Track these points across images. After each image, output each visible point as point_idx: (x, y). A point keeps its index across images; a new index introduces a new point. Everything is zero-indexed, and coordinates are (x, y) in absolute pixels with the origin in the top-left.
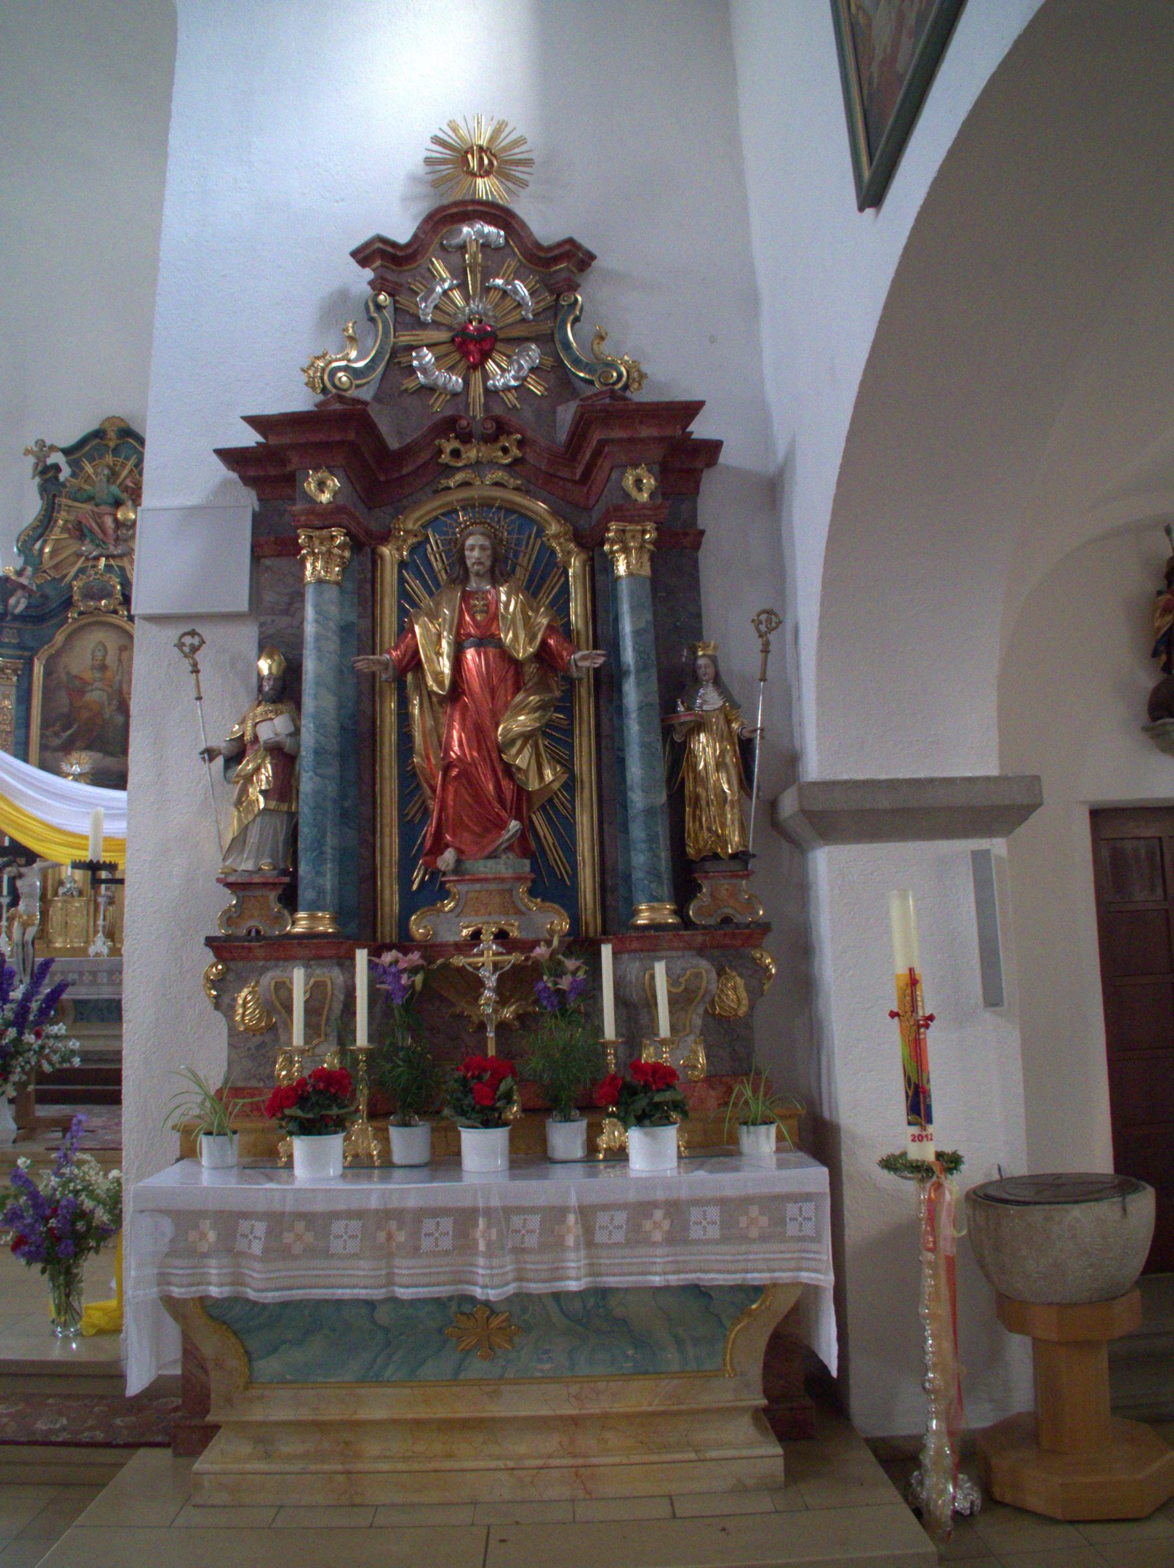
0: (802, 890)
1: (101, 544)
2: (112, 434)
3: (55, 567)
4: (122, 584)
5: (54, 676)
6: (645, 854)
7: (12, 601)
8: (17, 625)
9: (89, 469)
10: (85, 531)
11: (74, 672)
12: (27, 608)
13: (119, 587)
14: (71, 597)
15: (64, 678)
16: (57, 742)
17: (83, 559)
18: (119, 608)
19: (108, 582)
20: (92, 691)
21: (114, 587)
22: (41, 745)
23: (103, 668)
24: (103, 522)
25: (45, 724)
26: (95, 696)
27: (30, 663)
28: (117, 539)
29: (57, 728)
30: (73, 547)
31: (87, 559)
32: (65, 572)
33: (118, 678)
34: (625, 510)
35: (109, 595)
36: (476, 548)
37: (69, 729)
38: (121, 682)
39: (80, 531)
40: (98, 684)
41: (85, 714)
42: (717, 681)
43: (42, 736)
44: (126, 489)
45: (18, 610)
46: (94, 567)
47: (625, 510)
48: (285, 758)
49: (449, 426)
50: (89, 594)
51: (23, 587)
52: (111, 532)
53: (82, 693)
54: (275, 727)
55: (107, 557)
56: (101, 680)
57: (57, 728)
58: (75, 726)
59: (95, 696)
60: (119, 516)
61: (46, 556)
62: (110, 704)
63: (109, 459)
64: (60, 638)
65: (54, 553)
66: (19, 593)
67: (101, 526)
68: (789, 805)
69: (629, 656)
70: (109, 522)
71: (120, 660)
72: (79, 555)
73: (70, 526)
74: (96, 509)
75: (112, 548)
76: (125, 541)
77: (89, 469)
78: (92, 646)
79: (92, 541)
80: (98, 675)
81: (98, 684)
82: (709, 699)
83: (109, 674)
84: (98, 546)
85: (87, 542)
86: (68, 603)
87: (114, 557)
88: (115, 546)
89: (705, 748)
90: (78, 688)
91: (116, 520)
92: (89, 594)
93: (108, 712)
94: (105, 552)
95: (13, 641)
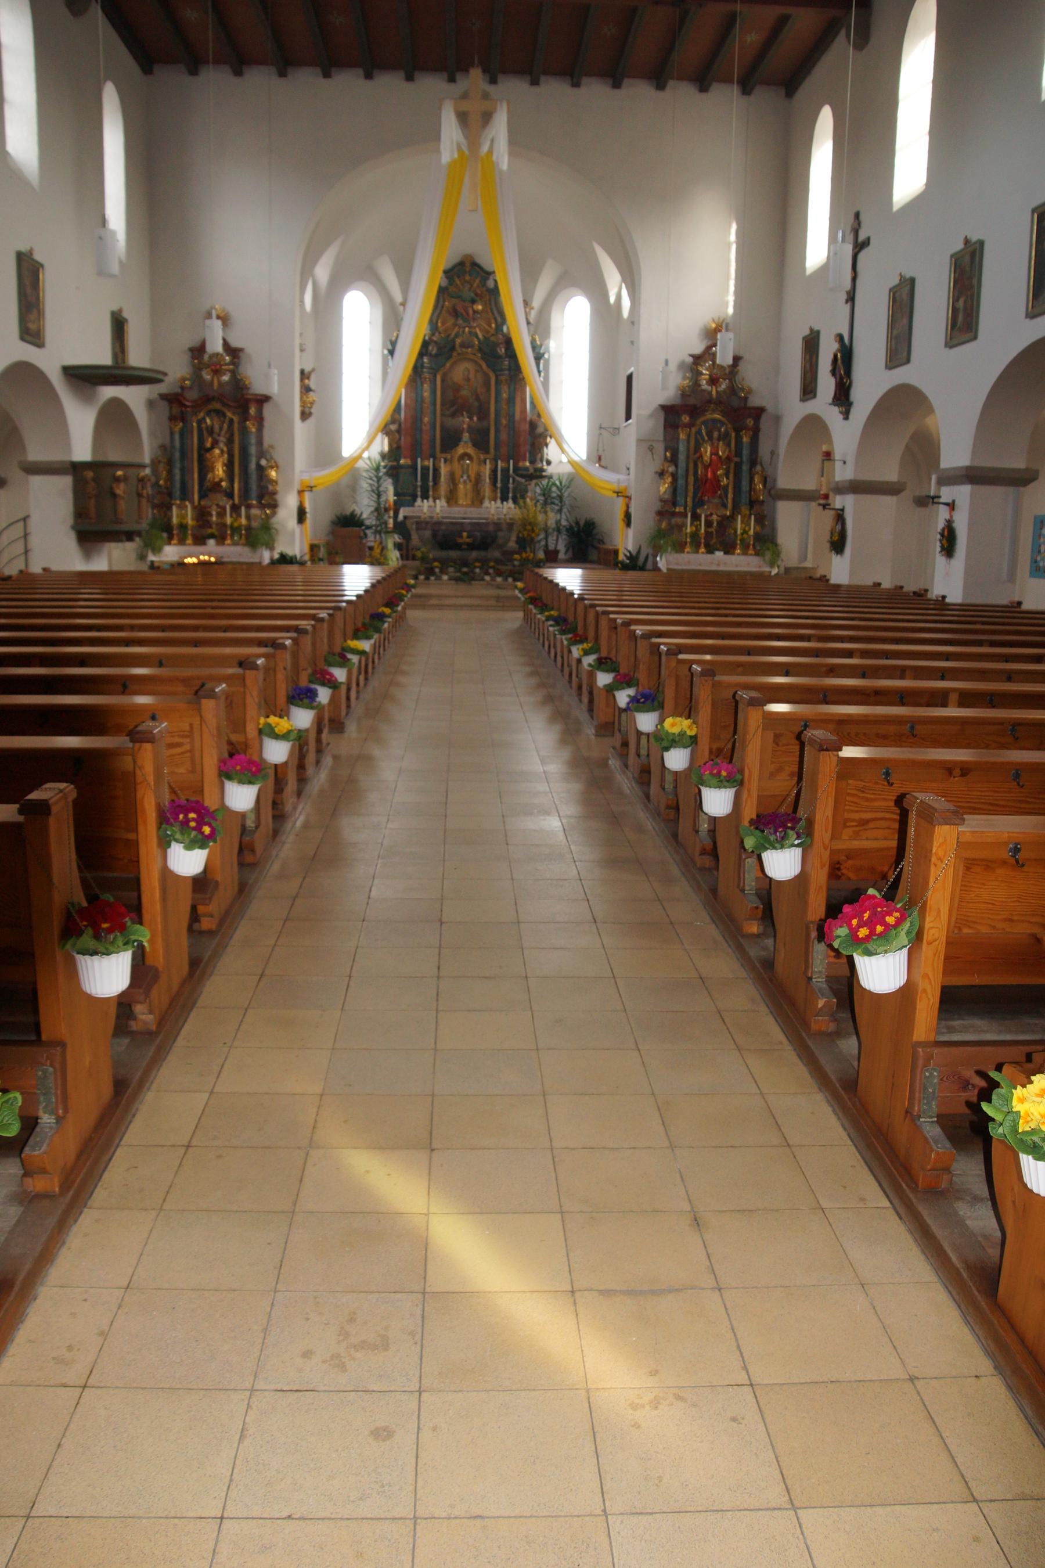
0: (774, 511)
1: (466, 320)
2: (468, 265)
6: (744, 499)
7: (430, 348)
9: (458, 282)
16: (448, 413)
23: (468, 380)
25: (443, 404)
26: (465, 393)
27: (435, 376)
30: (451, 321)
34: (747, 428)
35: (472, 346)
36: (716, 435)
39: (455, 313)
42: (761, 465)
44: (476, 294)
45: (434, 352)
46: (464, 332)
47: (747, 428)
48: (674, 476)
49: (710, 401)
50: (463, 345)
51: (435, 342)
54: (672, 469)
59: (465, 393)
61: (439, 324)
63: (467, 278)
64: (448, 365)
65: (443, 324)
67: (467, 312)
68: (773, 492)
69: (744, 459)
70: (471, 311)
77: (458, 282)
82: (758, 468)
86: (453, 349)
89: (757, 479)
90: (457, 388)
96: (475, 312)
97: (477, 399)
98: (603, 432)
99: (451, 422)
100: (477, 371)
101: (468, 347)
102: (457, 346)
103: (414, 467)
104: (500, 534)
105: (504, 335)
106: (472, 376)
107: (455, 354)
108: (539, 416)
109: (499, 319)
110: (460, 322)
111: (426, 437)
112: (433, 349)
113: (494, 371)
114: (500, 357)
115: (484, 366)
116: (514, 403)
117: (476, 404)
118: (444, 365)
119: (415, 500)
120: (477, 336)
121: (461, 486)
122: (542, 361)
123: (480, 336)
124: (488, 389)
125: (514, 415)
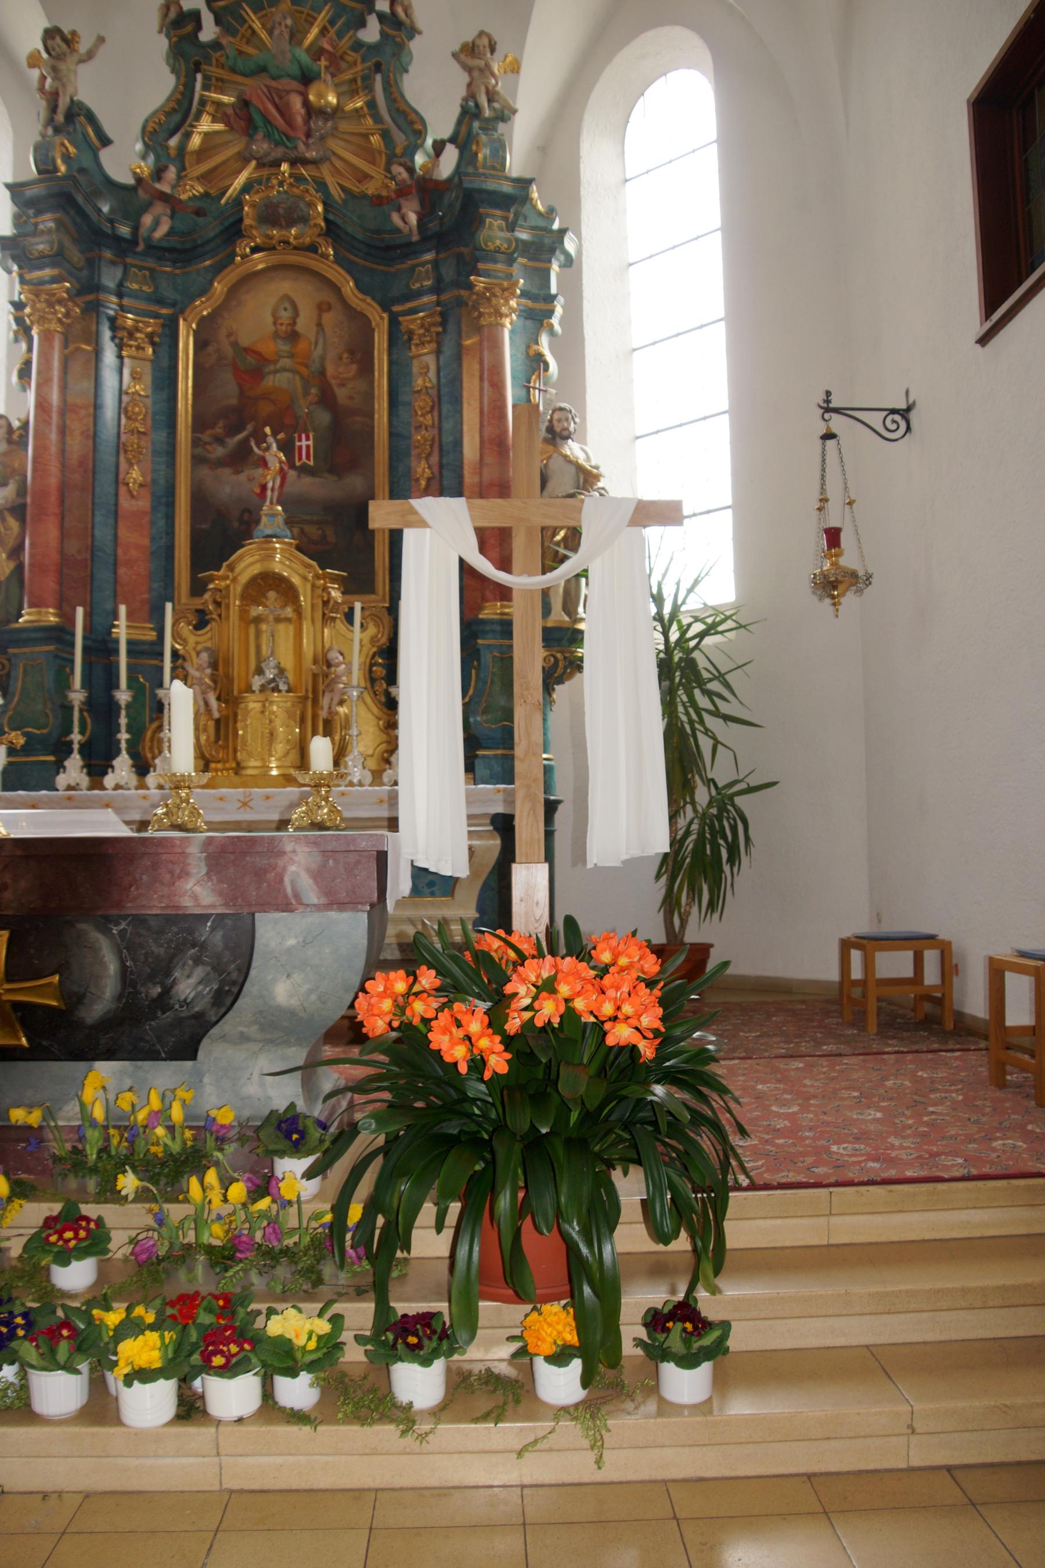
1: (283, 138)
3: (203, 178)
4: (325, 204)
5: (210, 349)
7: (147, 220)
8: (150, 263)
10: (258, 119)
11: (245, 342)
12: (171, 232)
13: (320, 208)
14: (241, 220)
15: (229, 351)
16: (219, 451)
17: (254, 163)
18: (320, 240)
19: (301, 198)
20: (276, 372)
21: (311, 205)
22: (193, 457)
23: (293, 336)
24: (287, 104)
25: (200, 423)
26: (278, 380)
28: (308, 135)
29: (219, 430)
31: (261, 165)
32: (221, 185)
33: (318, 352)
35: (304, 220)
37: (239, 432)
38: (323, 359)
40: (286, 362)
41: (265, 409)
43: (196, 442)
52: (299, 120)
53: (257, 374)
55: (293, 163)
56: (291, 356)
57: (219, 430)
58: (250, 428)
59: (278, 380)
60: (311, 98)
62: (306, 393)
64: (219, 287)
65: (203, 153)
66: (159, 208)
67: (284, 111)
71: (319, 325)
72: (244, 159)
73: (230, 111)
74: (274, 84)
75: (302, 147)
76: (322, 138)
78: (273, 301)
79: (268, 136)
80: (284, 347)
81: (286, 362)
83: (302, 346)
84: (277, 144)
85: (259, 136)
86: (234, 231)
87: (305, 162)
88: (307, 145)
90: (252, 367)
91: (306, 103)
92: (270, 216)
93: (303, 408)
94: (293, 155)
95: (145, 288)
96: (311, 111)
97: (326, 398)
98: (837, 423)
99: (229, 486)
100: (322, 308)
101: (290, 224)
102: (247, 222)
103: (61, 634)
104: (273, 932)
105: (411, 170)
106: (305, 324)
107: (244, 247)
108: (557, 435)
109: (400, 139)
110: (261, 146)
111: (134, 540)
112: (157, 224)
113: (385, 306)
114: (407, 249)
115: (349, 287)
116: (457, 401)
117: (324, 417)
118: (205, 290)
119: (59, 766)
120: (321, 186)
121: (253, 704)
122: (555, 267)
123: (336, 192)
124: (366, 367)
125: (458, 444)
